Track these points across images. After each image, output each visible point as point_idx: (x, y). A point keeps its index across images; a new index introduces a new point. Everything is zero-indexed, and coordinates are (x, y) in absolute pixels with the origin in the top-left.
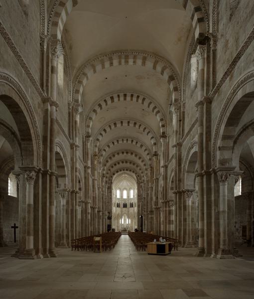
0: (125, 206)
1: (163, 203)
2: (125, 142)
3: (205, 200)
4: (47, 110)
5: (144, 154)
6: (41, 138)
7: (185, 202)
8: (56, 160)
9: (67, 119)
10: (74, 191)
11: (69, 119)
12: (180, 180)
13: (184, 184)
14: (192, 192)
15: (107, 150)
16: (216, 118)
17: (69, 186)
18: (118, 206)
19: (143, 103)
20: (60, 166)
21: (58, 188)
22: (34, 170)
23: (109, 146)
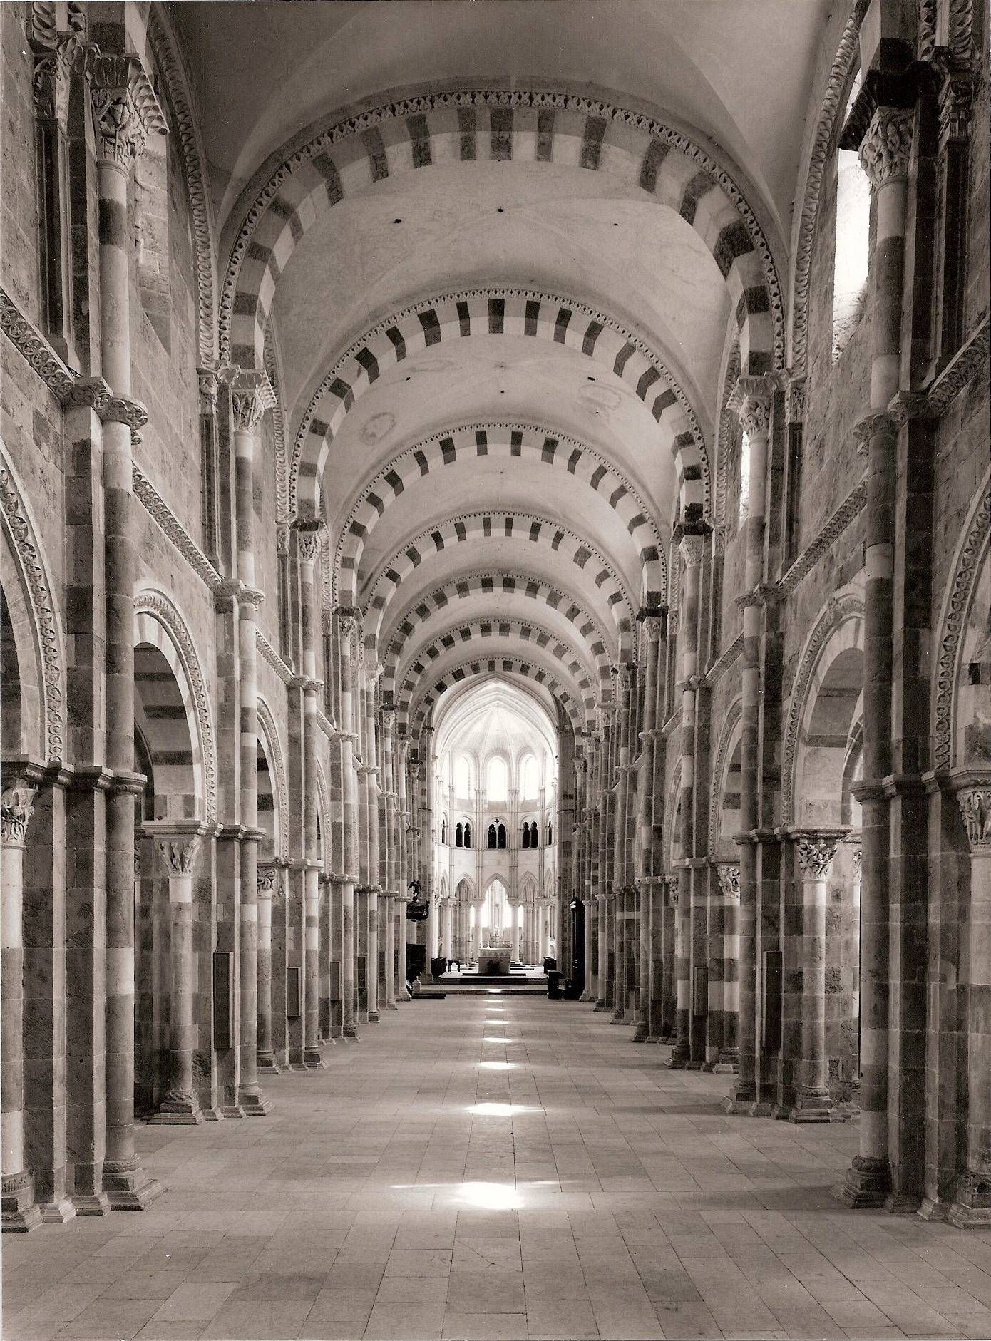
0: (497, 839)
1: (687, 870)
2: (498, 531)
3: (896, 923)
4: (83, 448)
5: (596, 598)
6: (56, 600)
7: (795, 890)
8: (138, 677)
9: (195, 454)
10: (236, 831)
11: (207, 454)
12: (772, 779)
13: (790, 796)
14: (831, 839)
15: (403, 577)
16: (961, 513)
17: (208, 811)
18: (463, 838)
19: (588, 350)
20: (162, 709)
21: (150, 817)
22: (25, 777)
23: (413, 555)
